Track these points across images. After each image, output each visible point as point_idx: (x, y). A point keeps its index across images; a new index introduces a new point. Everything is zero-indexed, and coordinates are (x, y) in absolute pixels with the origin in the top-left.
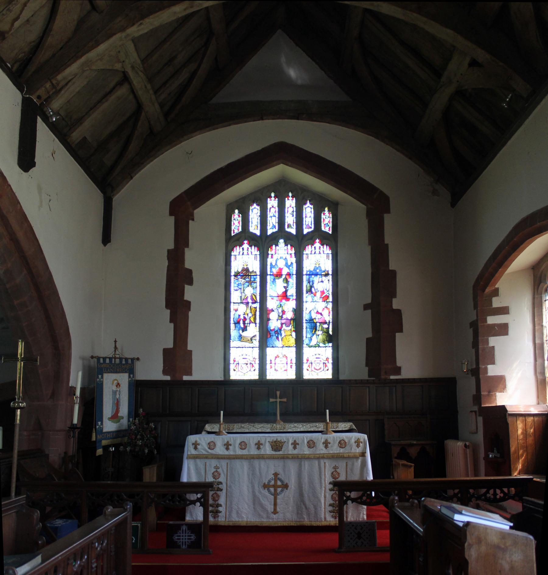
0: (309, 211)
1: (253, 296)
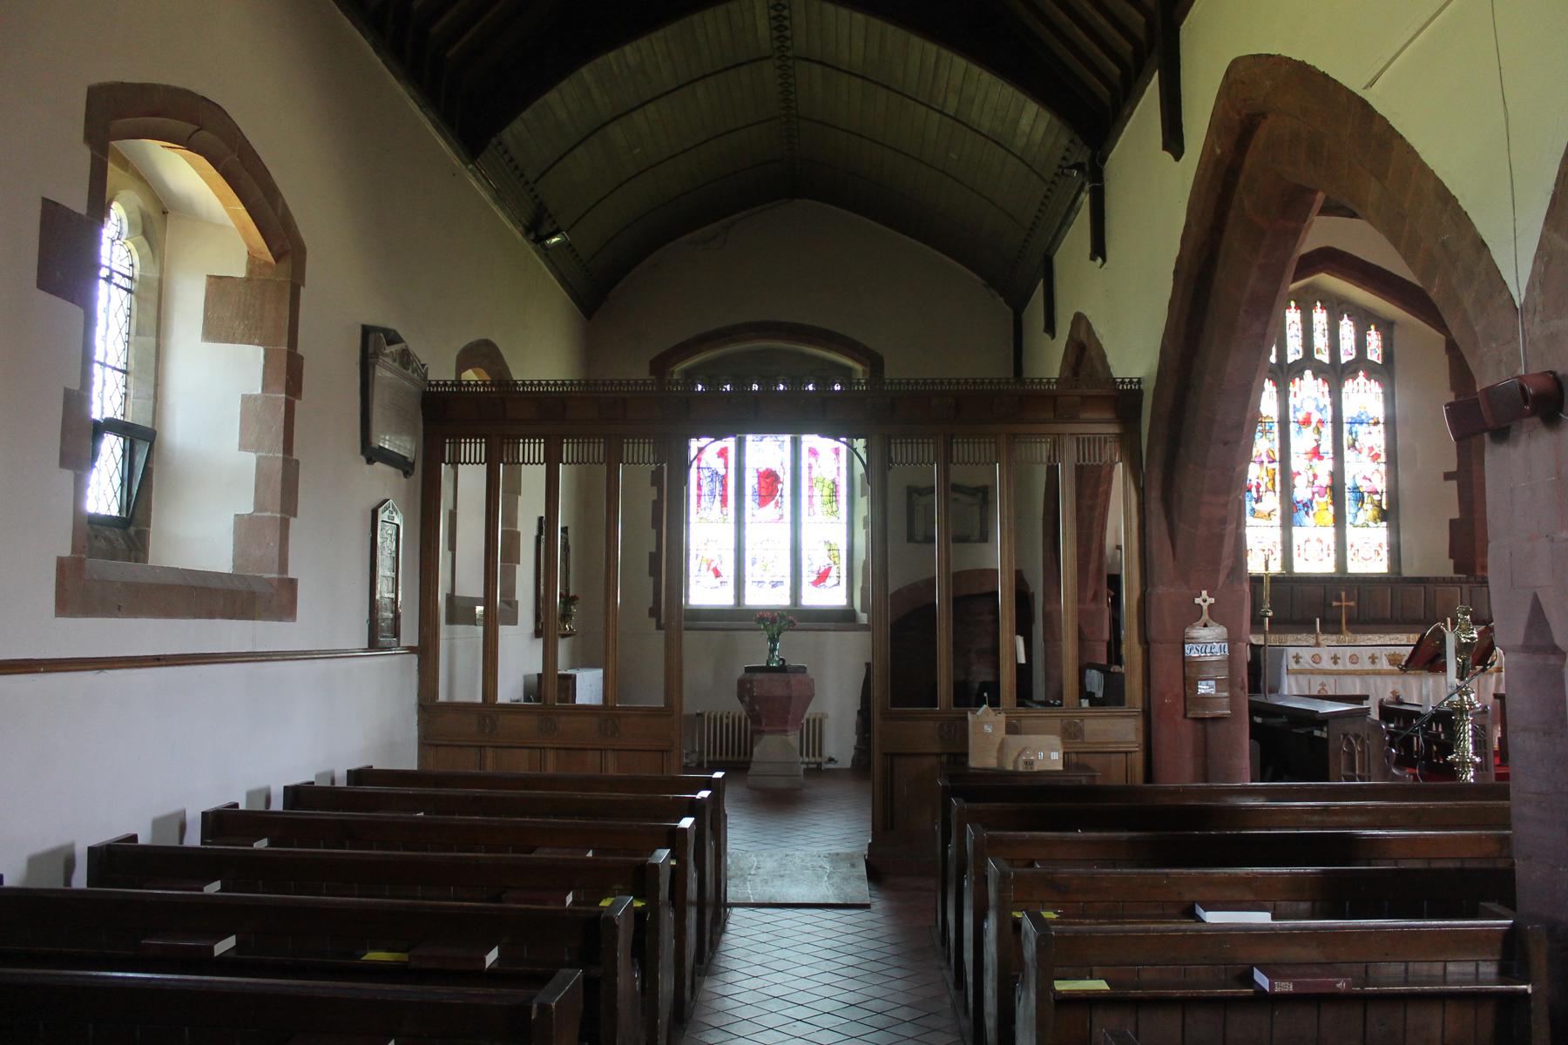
0: (1347, 328)
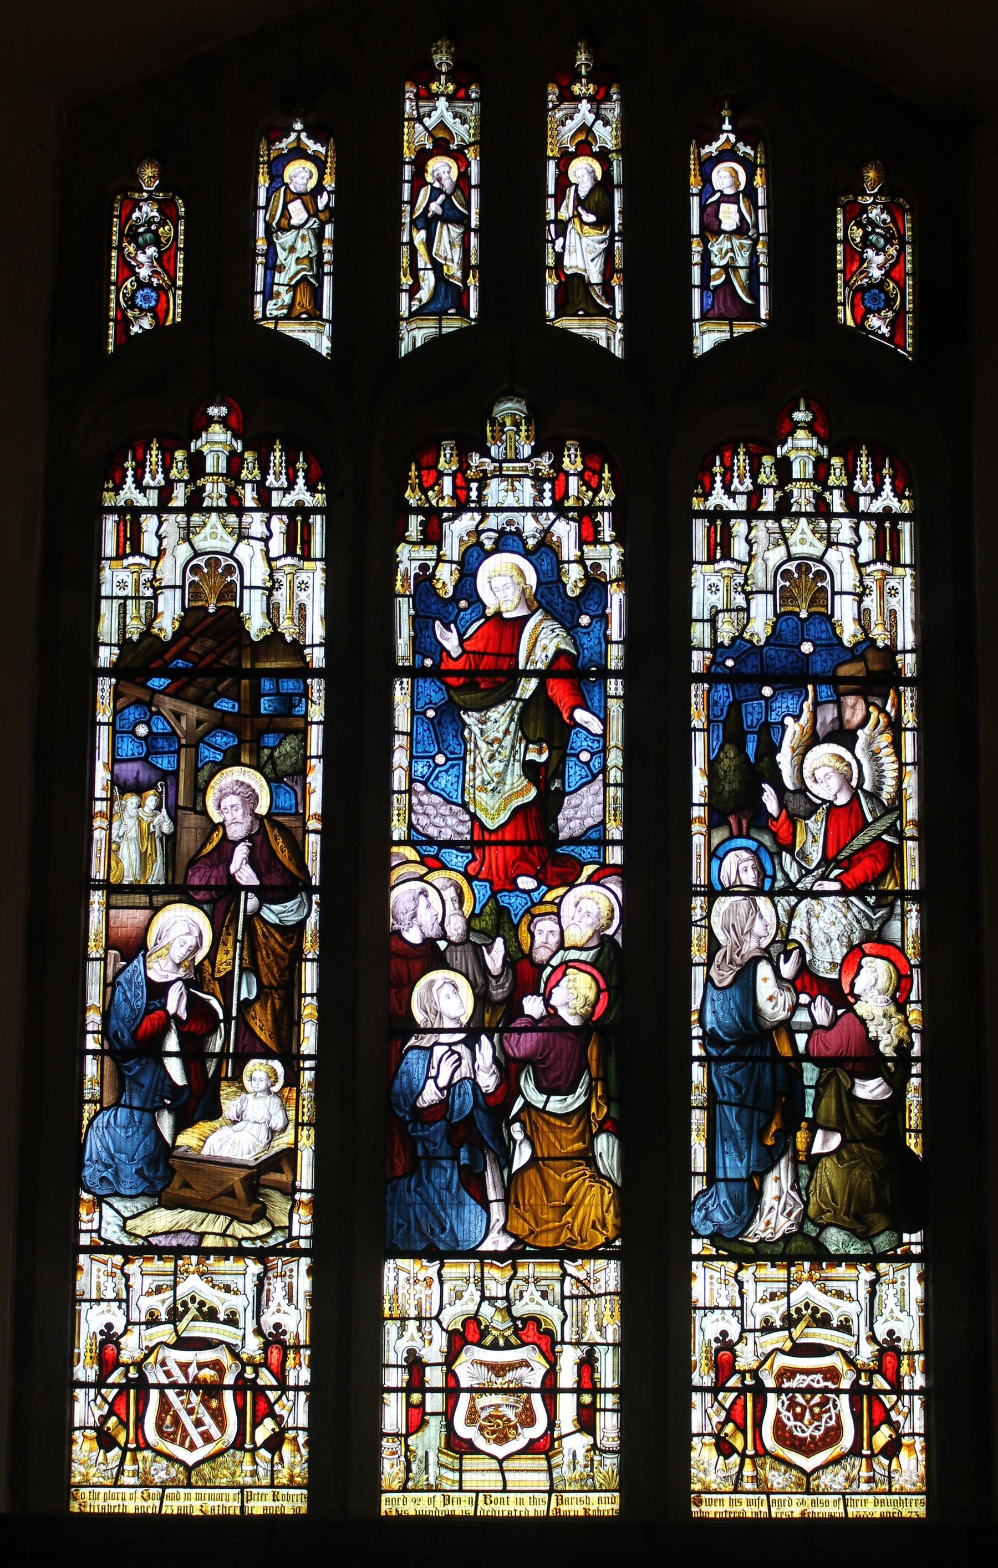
1: (272, 833)
